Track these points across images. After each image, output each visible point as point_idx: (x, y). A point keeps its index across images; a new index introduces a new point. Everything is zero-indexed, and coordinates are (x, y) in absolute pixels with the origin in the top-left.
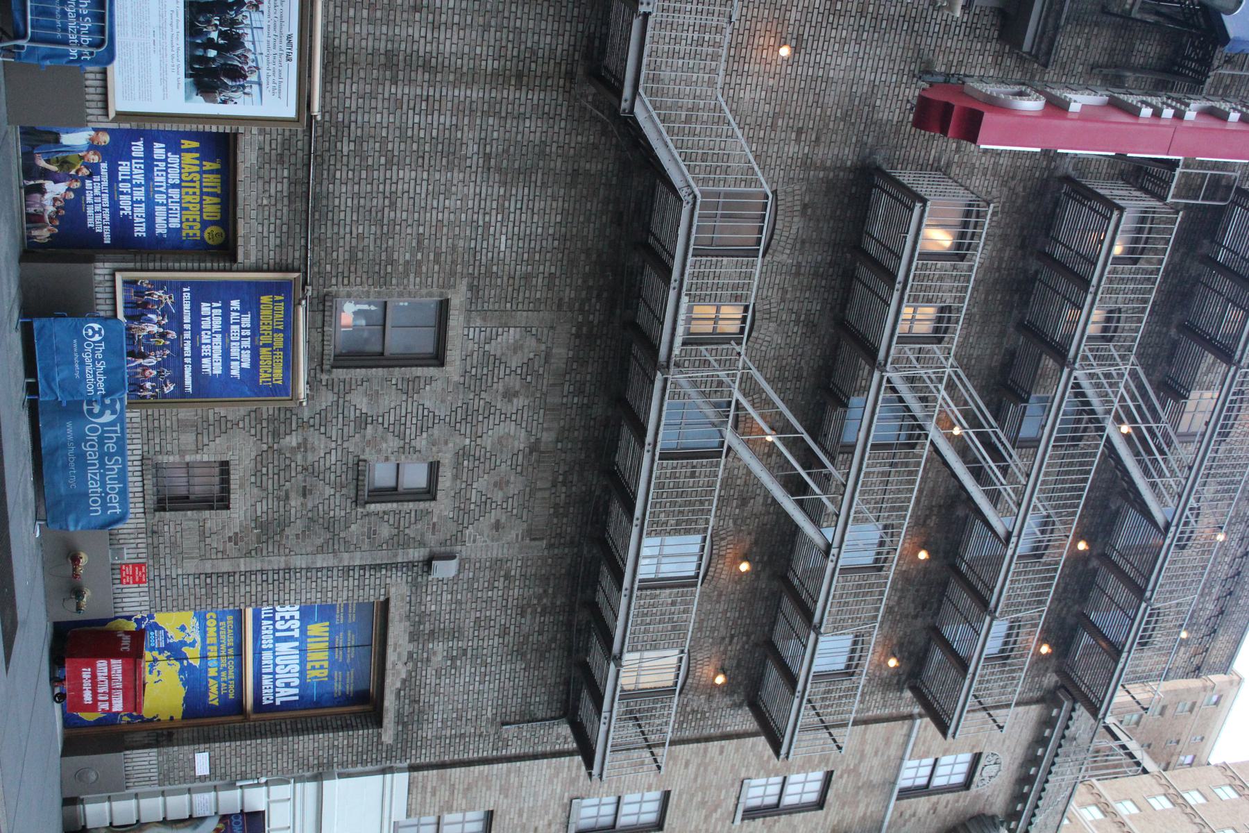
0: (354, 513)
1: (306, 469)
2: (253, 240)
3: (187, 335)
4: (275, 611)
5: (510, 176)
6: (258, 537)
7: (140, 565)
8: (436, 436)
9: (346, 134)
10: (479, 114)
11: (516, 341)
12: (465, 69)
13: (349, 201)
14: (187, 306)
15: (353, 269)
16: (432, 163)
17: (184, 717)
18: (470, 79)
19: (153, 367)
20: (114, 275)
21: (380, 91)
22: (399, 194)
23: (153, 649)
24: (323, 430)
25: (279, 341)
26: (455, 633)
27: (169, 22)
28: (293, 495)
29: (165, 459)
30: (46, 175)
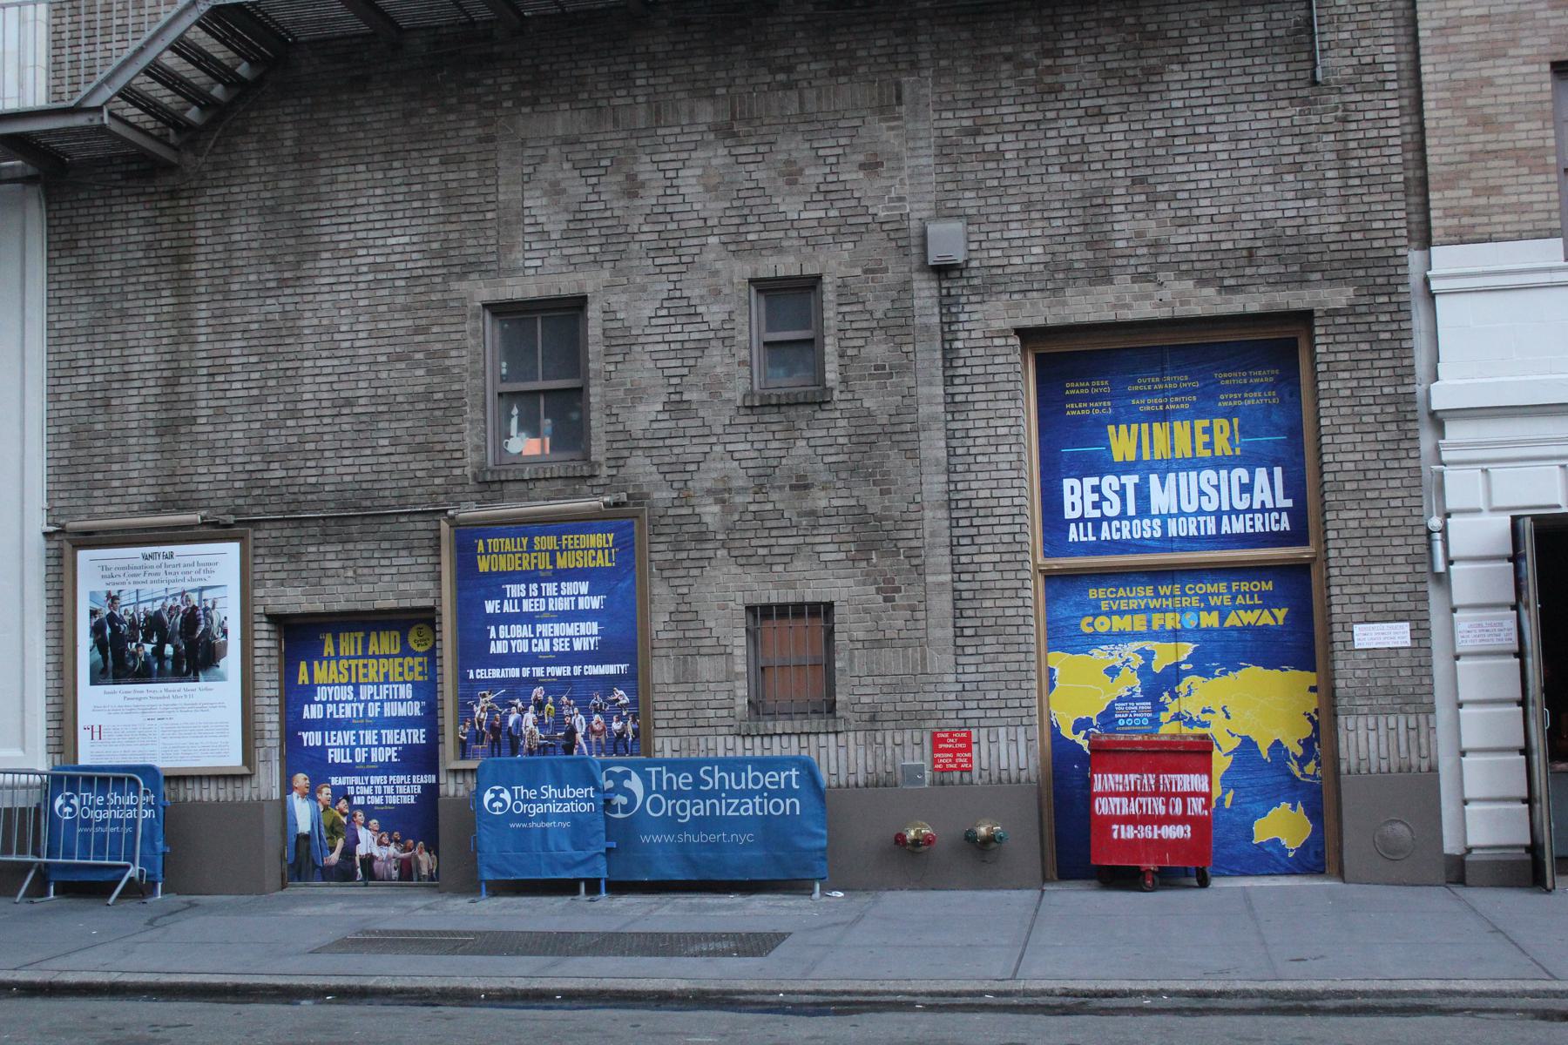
0: (842, 406)
1: (762, 486)
2: (402, 587)
3: (539, 672)
4: (1082, 519)
5: (306, 248)
6: (884, 554)
7: (936, 741)
8: (704, 292)
9: (259, 475)
10: (227, 304)
11: (545, 193)
12: (174, 332)
13: (346, 461)
14: (496, 673)
15: (439, 447)
16: (292, 356)
17: (1314, 670)
18: (185, 324)
19: (589, 720)
20: (455, 772)
21: (204, 437)
22: (335, 395)
23: (1155, 722)
24: (693, 467)
25: (550, 542)
26: (1095, 205)
27: (136, 702)
28: (807, 505)
29: (742, 702)
30: (348, 852)
